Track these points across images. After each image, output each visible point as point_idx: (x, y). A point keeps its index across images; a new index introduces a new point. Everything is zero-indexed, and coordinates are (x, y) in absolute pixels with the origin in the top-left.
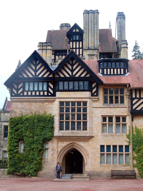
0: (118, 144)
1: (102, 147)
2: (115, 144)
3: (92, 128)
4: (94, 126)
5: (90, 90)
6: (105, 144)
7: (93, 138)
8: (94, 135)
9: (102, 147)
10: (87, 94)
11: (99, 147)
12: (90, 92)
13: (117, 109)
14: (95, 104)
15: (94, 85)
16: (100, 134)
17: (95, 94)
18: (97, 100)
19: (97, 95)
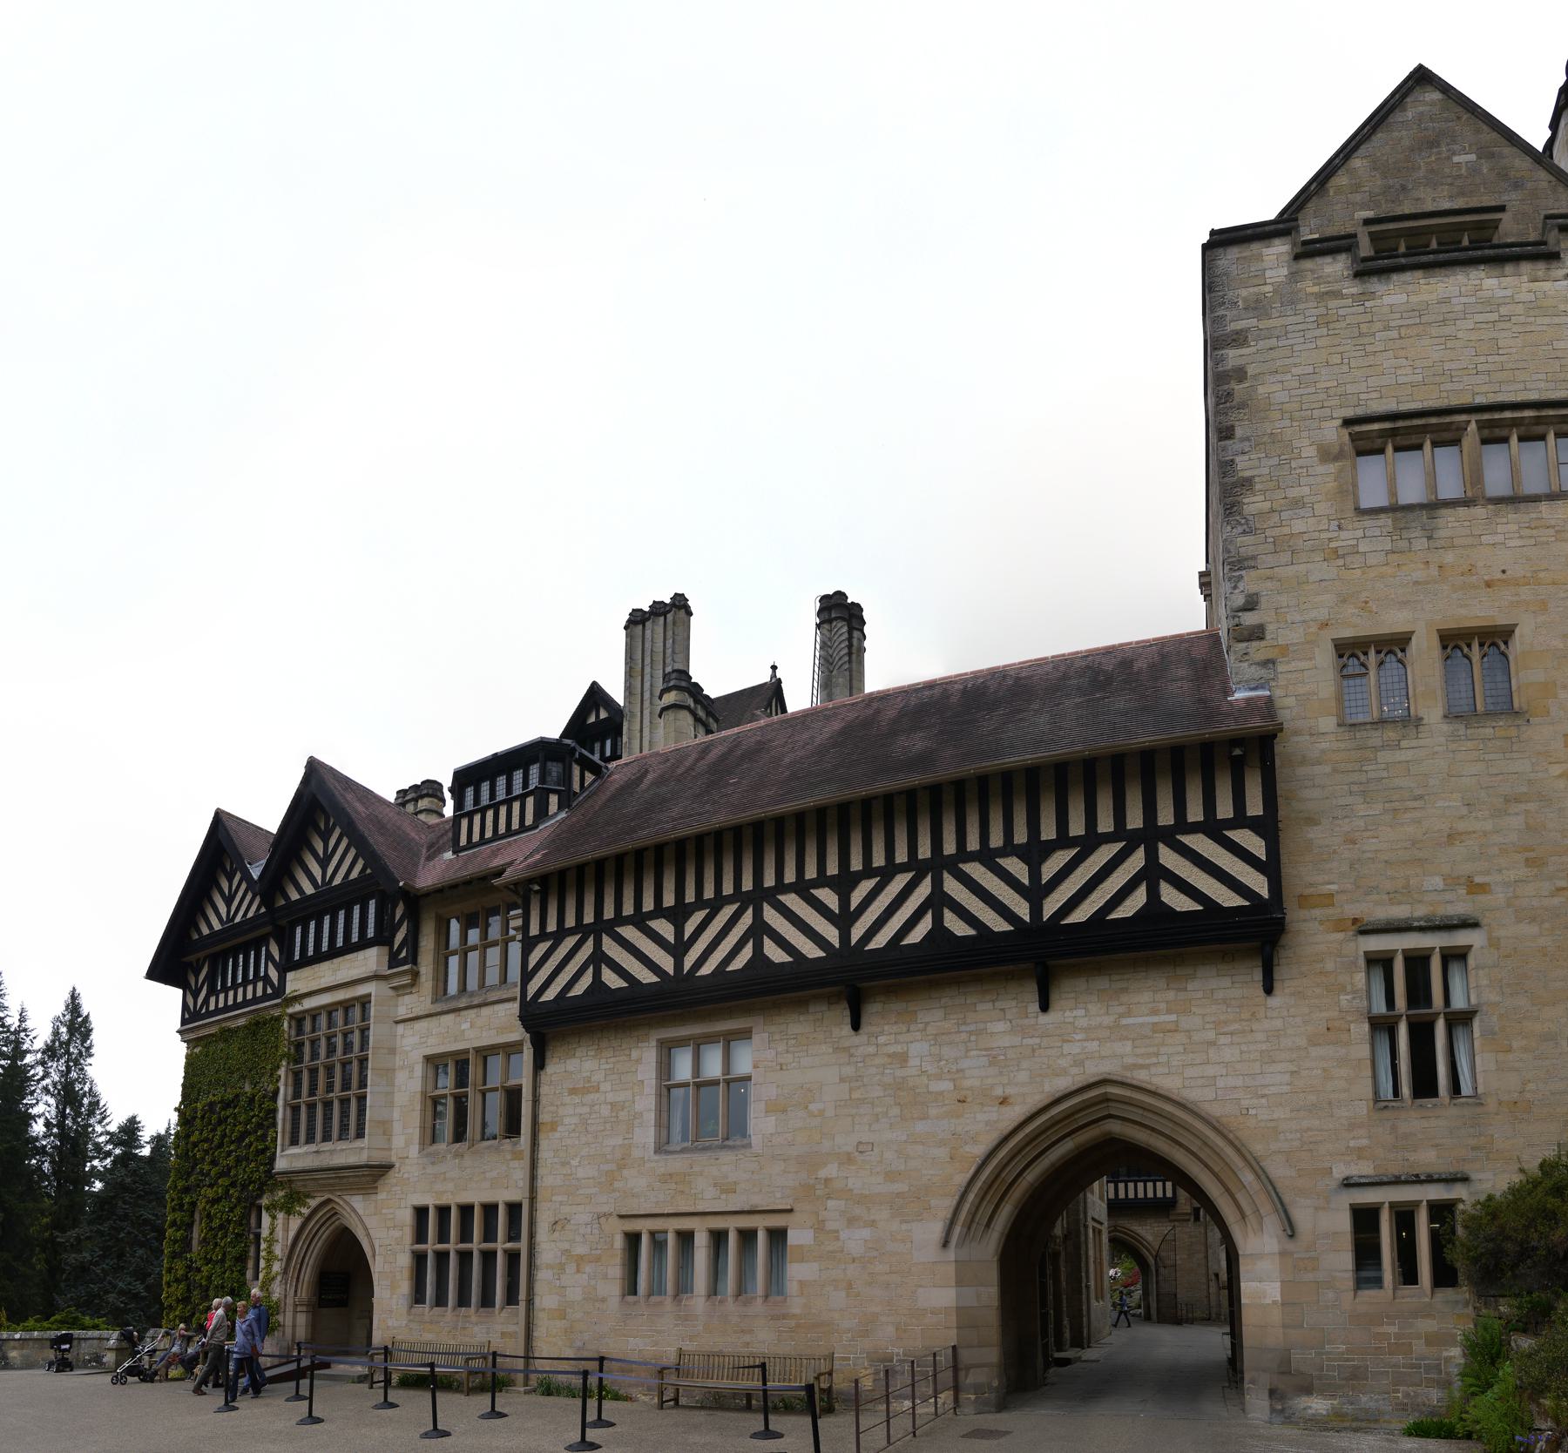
0: (476, 1196)
1: (421, 1213)
2: (443, 1201)
3: (385, 1127)
4: (396, 1115)
5: (383, 938)
6: (430, 1201)
7: (392, 1171)
8: (394, 1159)
9: (421, 1213)
10: (370, 960)
11: (407, 1217)
12: (385, 949)
13: (485, 1011)
14: (410, 1004)
15: (399, 913)
16: (414, 1150)
17: (403, 954)
18: (406, 980)
19: (413, 958)
